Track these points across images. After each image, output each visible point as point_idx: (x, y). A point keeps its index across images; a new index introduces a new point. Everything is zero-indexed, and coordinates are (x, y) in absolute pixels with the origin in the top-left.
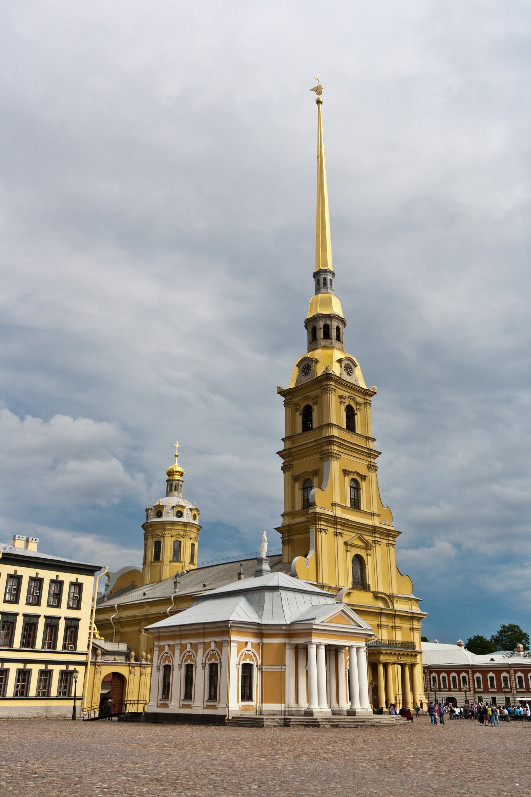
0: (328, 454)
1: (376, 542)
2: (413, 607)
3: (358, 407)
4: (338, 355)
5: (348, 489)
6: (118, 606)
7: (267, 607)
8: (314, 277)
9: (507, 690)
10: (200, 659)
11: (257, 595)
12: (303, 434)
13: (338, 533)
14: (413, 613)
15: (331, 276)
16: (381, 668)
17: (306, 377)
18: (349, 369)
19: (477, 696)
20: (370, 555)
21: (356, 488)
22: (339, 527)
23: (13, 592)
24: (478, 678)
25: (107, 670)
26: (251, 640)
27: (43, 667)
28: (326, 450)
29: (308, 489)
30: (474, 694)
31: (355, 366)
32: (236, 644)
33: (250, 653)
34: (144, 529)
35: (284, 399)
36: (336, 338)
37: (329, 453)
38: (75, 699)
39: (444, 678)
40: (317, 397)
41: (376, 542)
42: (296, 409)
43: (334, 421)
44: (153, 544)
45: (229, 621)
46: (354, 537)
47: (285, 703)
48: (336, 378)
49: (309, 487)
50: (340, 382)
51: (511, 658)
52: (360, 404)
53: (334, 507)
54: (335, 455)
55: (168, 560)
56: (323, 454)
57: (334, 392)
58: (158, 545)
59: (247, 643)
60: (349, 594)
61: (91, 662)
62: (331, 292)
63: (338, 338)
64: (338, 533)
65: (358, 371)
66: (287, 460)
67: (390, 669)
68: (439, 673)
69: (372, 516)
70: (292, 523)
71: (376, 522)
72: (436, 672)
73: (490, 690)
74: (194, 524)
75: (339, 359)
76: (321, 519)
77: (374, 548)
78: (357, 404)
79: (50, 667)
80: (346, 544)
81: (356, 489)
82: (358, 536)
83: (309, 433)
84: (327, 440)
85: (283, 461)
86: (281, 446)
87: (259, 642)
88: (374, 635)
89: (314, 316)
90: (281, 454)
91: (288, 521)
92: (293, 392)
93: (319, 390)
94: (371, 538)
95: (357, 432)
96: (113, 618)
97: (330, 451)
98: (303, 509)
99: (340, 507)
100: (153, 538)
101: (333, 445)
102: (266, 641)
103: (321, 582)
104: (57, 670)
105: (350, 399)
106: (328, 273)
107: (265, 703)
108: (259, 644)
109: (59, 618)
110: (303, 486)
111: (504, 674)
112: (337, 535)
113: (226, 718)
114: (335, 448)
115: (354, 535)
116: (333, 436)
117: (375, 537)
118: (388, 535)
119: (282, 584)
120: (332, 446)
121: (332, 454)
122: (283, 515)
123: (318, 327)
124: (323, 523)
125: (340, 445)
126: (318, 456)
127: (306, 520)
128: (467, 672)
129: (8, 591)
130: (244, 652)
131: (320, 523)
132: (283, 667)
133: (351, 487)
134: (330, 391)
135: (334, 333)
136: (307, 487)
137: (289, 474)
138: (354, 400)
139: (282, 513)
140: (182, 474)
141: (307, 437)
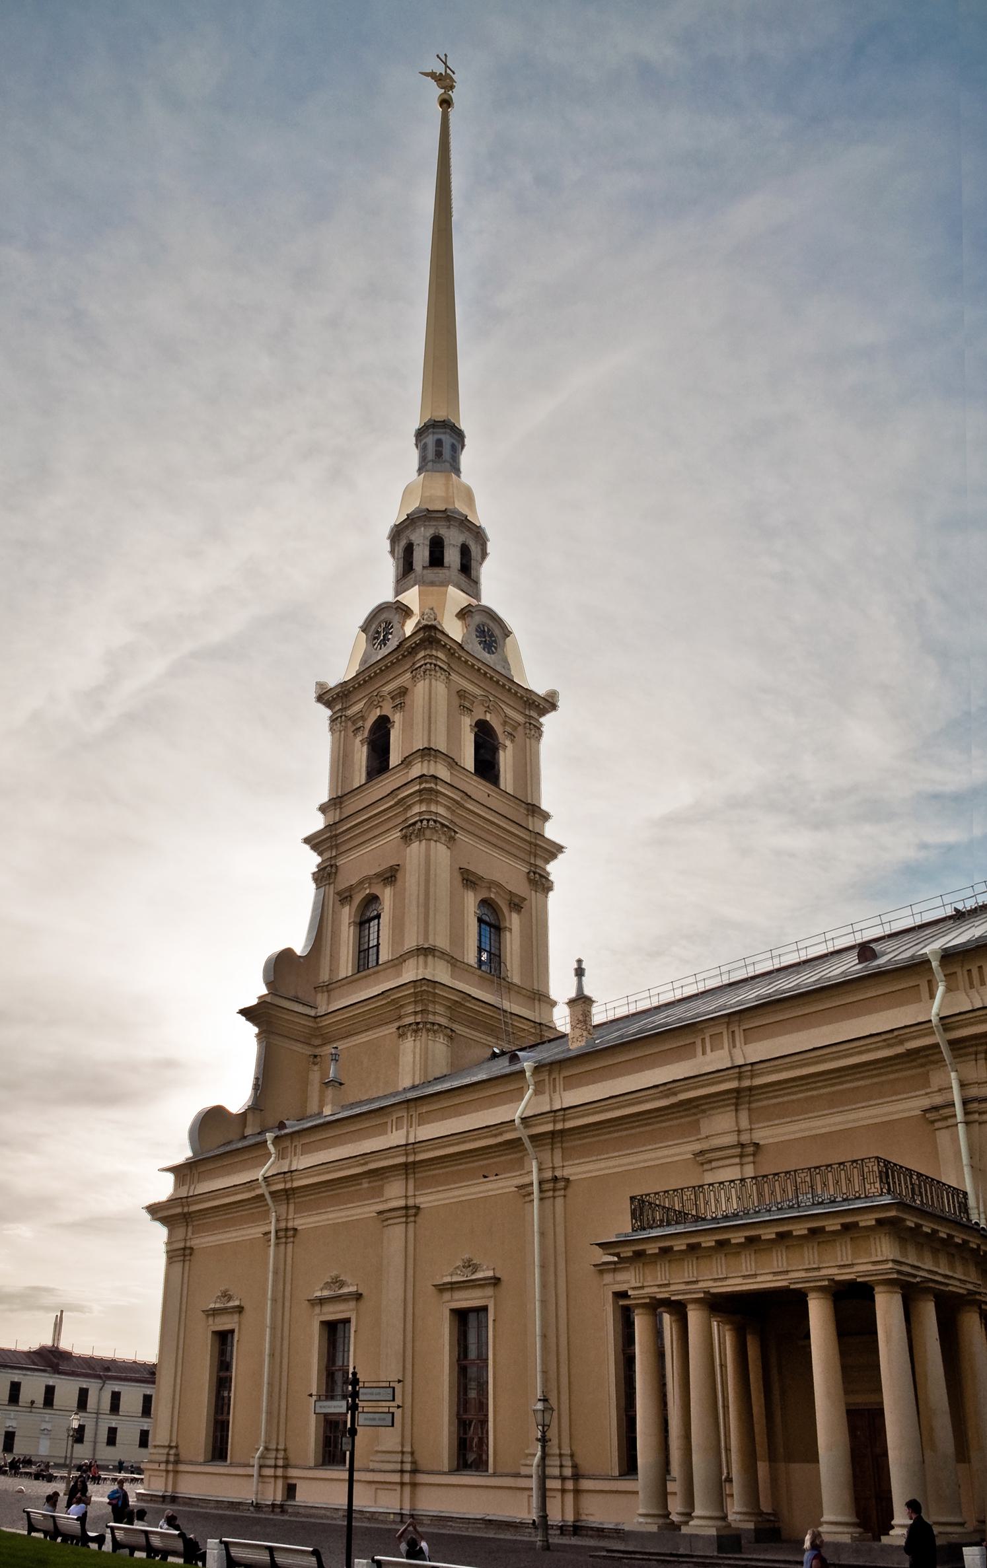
0: (419, 824)
12: (366, 786)
15: (455, 439)
29: (372, 924)
36: (459, 566)
37: (421, 821)
40: (403, 692)
42: (353, 732)
50: (459, 658)
57: (442, 677)
66: (327, 855)
75: (462, 609)
84: (417, 788)
90: (313, 843)
92: (350, 692)
93: (408, 675)
101: (437, 802)
106: (449, 431)
110: (362, 914)
126: (396, 834)
134: (433, 673)
135: (452, 556)
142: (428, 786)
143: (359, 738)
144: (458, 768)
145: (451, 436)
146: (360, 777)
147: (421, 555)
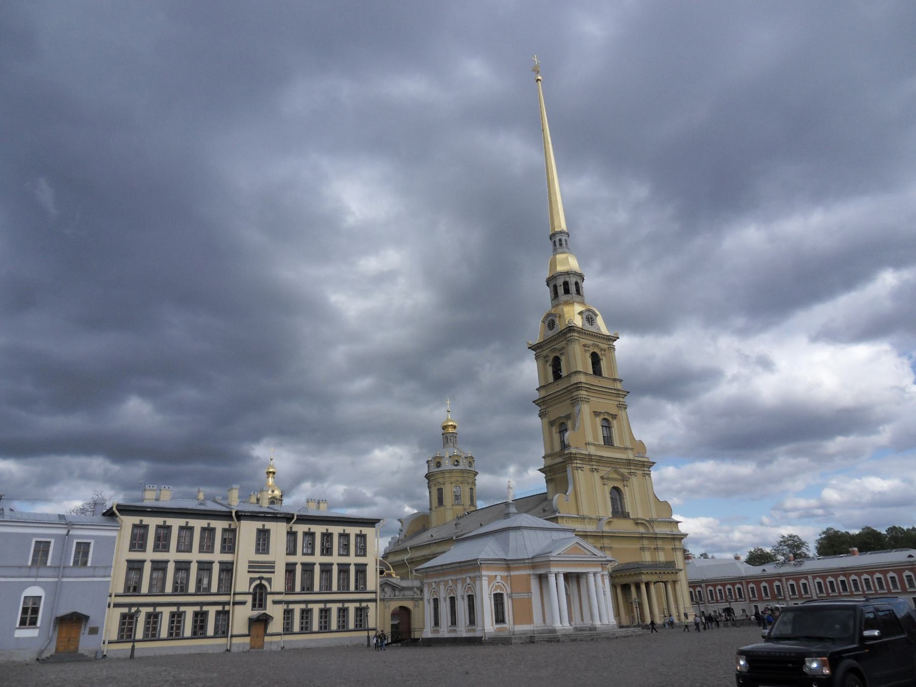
1: (632, 474)
2: (673, 529)
3: (603, 352)
4: (578, 308)
5: (600, 428)
6: (410, 548)
7: (512, 544)
8: (551, 239)
9: (780, 598)
10: (460, 592)
11: (503, 535)
13: (594, 470)
14: (674, 535)
16: (643, 587)
17: (552, 331)
18: (590, 320)
19: (752, 605)
20: (627, 486)
21: (607, 426)
22: (594, 463)
23: (309, 546)
24: (752, 588)
25: (395, 605)
26: (500, 574)
27: (340, 605)
28: (575, 396)
30: (749, 603)
31: (596, 315)
32: (487, 578)
33: (500, 584)
34: (427, 478)
35: (535, 353)
36: (575, 292)
38: (368, 630)
39: (720, 590)
40: (563, 348)
41: (632, 474)
43: (580, 369)
44: (436, 491)
45: (478, 559)
46: (609, 471)
47: (533, 623)
48: (578, 329)
49: (564, 430)
51: (782, 568)
53: (588, 446)
55: (451, 504)
56: (573, 400)
58: (440, 491)
59: (496, 576)
60: (609, 523)
61: (380, 599)
62: (567, 251)
63: (578, 292)
64: (594, 470)
65: (600, 321)
66: (542, 408)
67: (652, 587)
68: (715, 586)
69: (626, 451)
70: (552, 464)
71: (630, 455)
72: (712, 585)
73: (764, 599)
74: (470, 470)
76: (576, 458)
77: (631, 479)
79: (346, 605)
80: (602, 478)
81: (608, 427)
82: (613, 470)
83: (560, 382)
85: (539, 409)
86: (537, 395)
87: (507, 574)
88: (614, 561)
89: (553, 275)
91: (550, 462)
93: (565, 342)
94: (627, 471)
96: (406, 559)
97: (579, 396)
98: (562, 450)
100: (435, 486)
101: (582, 390)
102: (512, 573)
103: (582, 514)
104: (352, 607)
107: (517, 624)
108: (507, 576)
109: (350, 564)
111: (777, 583)
112: (593, 471)
113: (483, 639)
114: (584, 393)
115: (609, 470)
116: (581, 382)
117: (630, 469)
118: (644, 466)
119: (524, 524)
120: (581, 391)
121: (581, 399)
122: (543, 457)
123: (558, 285)
124: (578, 462)
125: (588, 389)
127: (564, 460)
128: (741, 583)
129: (305, 546)
130: (493, 585)
131: (575, 462)
132: (530, 594)
133: (602, 426)
135: (573, 288)
136: (563, 430)
137: (546, 420)
138: (598, 346)
139: (543, 455)
140: (455, 427)
141: (558, 385)
142: (578, 385)
143: (549, 364)
146: (551, 379)
147: (561, 290)
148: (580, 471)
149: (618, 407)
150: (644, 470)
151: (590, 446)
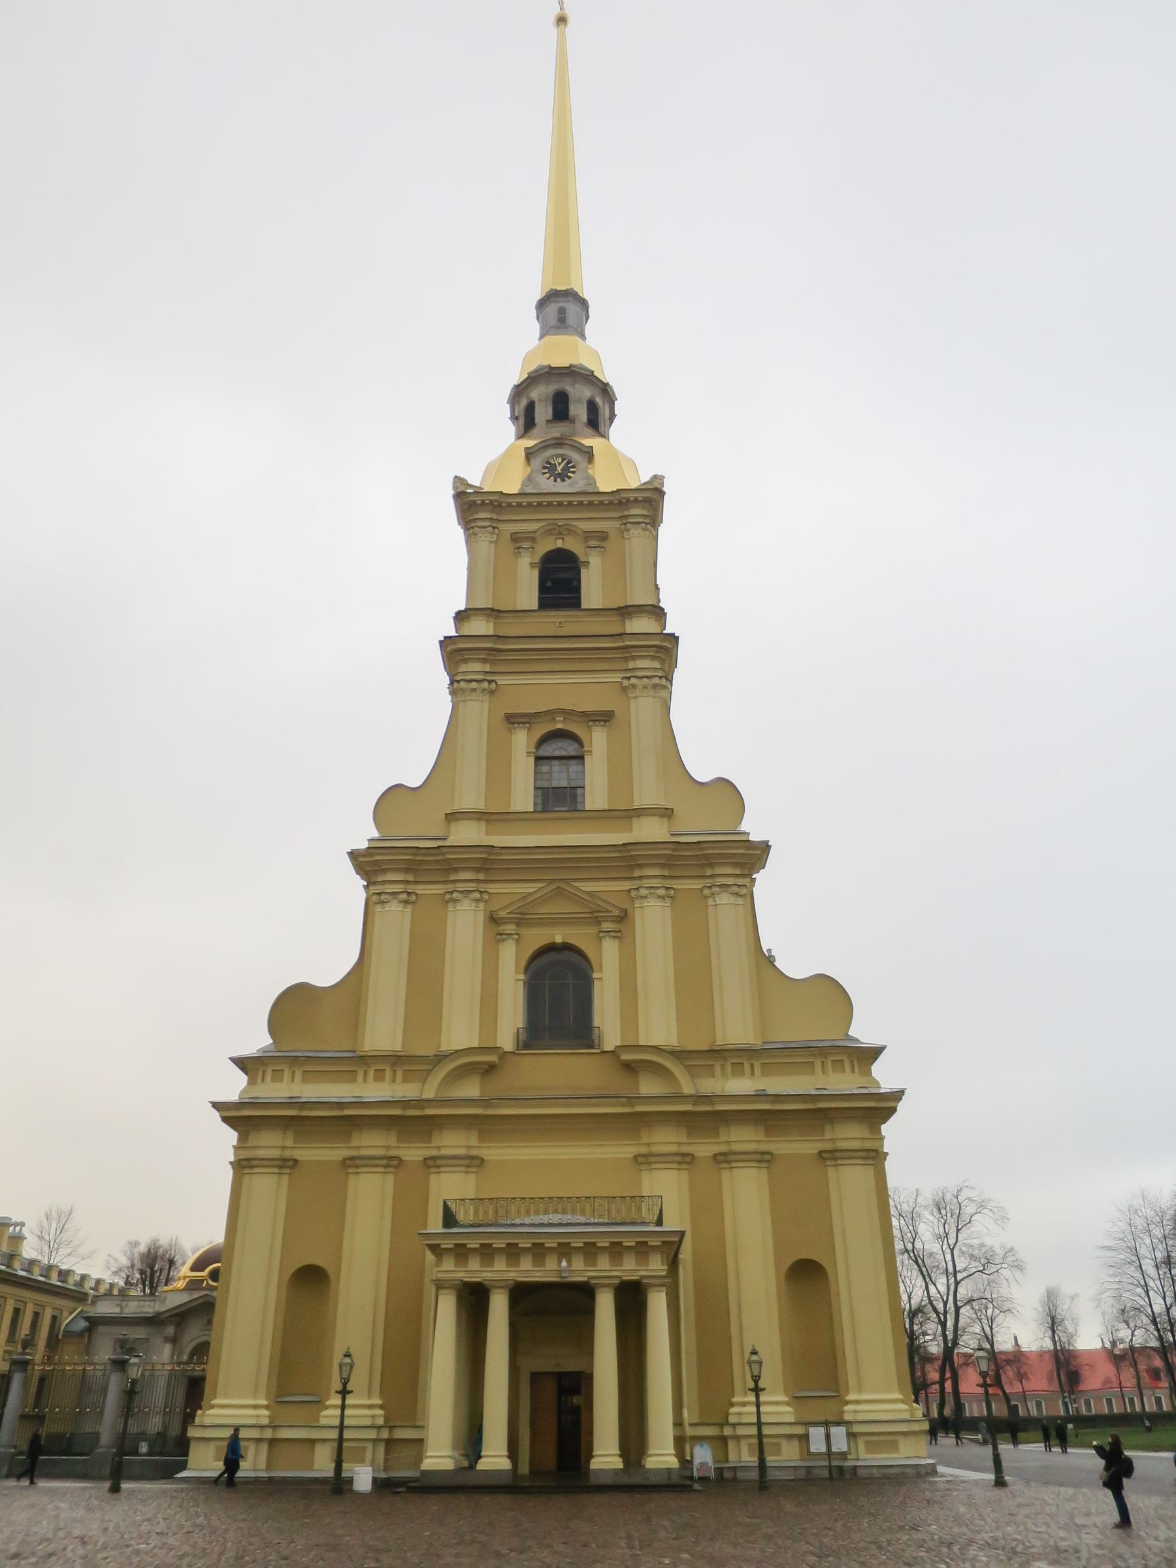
3: (593, 543)
48: (487, 500)
50: (509, 505)
52: (603, 536)
54: (463, 684)
64: (455, 895)
69: (635, 821)
71: (650, 830)
77: (638, 913)
78: (588, 536)
80: (493, 920)
95: (583, 606)
99: (479, 819)
105: (560, 533)
112: (455, 901)
117: (640, 878)
124: (390, 877)
131: (380, 879)
138: (571, 531)
144: (501, 614)
145: (555, 302)
148: (394, 907)
149: (625, 689)
150: (711, 876)
151: (459, 822)
